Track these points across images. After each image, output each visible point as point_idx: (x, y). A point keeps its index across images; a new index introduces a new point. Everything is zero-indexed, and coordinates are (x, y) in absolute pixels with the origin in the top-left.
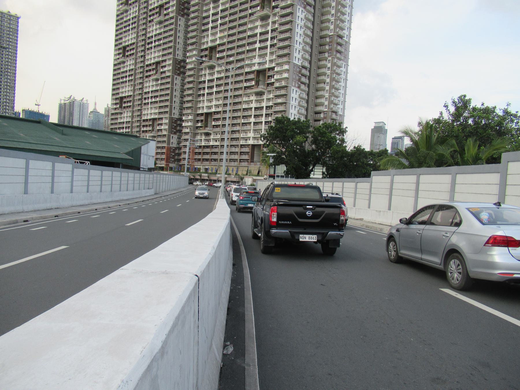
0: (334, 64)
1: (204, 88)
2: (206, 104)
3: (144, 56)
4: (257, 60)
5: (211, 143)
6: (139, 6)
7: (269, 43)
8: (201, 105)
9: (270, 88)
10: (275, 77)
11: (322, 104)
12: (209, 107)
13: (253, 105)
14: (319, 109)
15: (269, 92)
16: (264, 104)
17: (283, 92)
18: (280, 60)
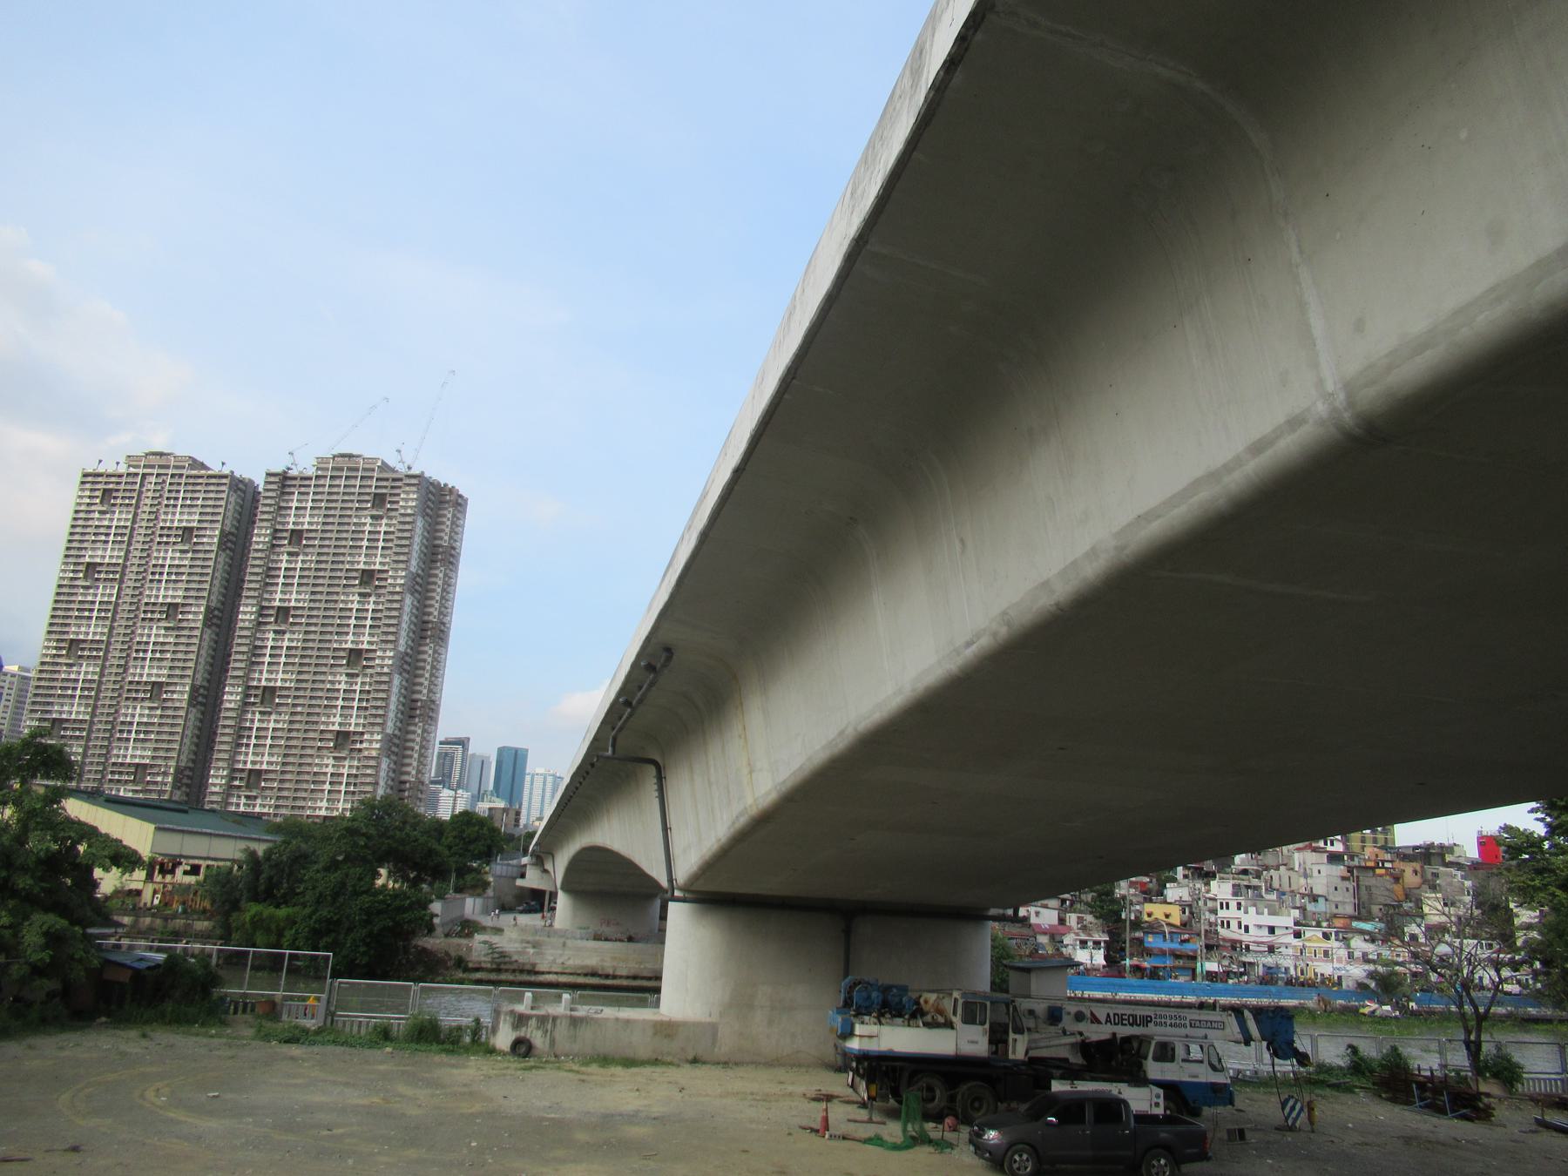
0: (424, 731)
1: (249, 737)
2: (250, 758)
3: (125, 668)
4: (338, 719)
5: (257, 809)
6: (120, 589)
7: (356, 704)
8: (242, 758)
9: (355, 754)
10: (365, 745)
11: (408, 773)
12: (254, 763)
13: (330, 770)
14: (405, 778)
15: (352, 758)
16: (345, 771)
17: (372, 763)
18: (370, 729)
